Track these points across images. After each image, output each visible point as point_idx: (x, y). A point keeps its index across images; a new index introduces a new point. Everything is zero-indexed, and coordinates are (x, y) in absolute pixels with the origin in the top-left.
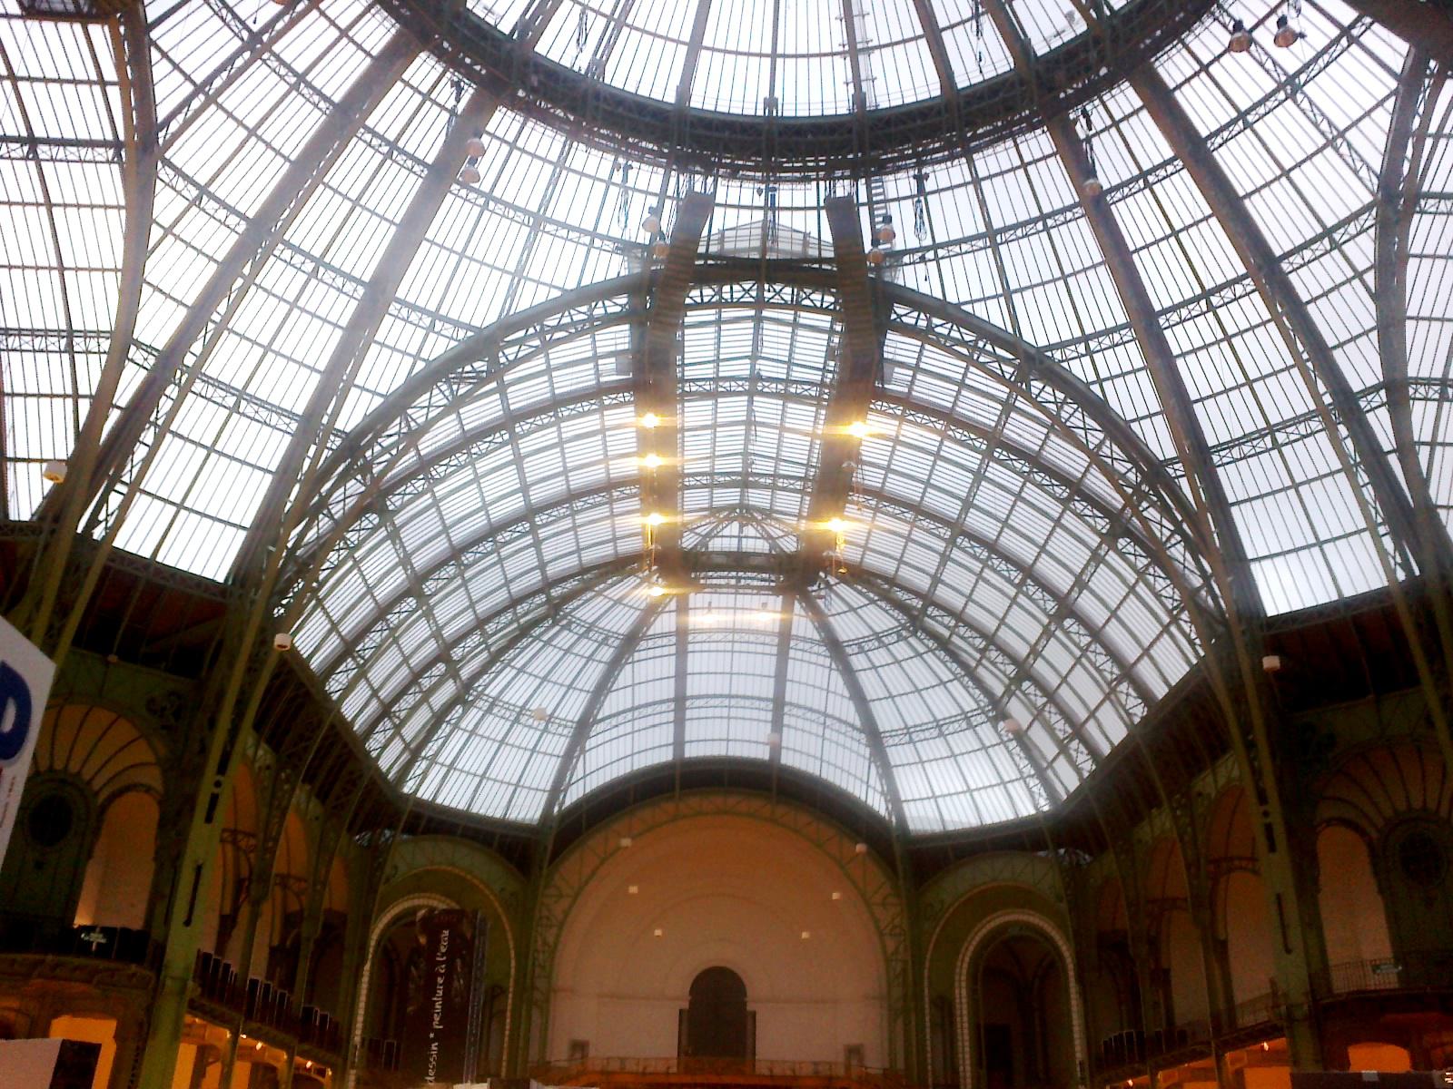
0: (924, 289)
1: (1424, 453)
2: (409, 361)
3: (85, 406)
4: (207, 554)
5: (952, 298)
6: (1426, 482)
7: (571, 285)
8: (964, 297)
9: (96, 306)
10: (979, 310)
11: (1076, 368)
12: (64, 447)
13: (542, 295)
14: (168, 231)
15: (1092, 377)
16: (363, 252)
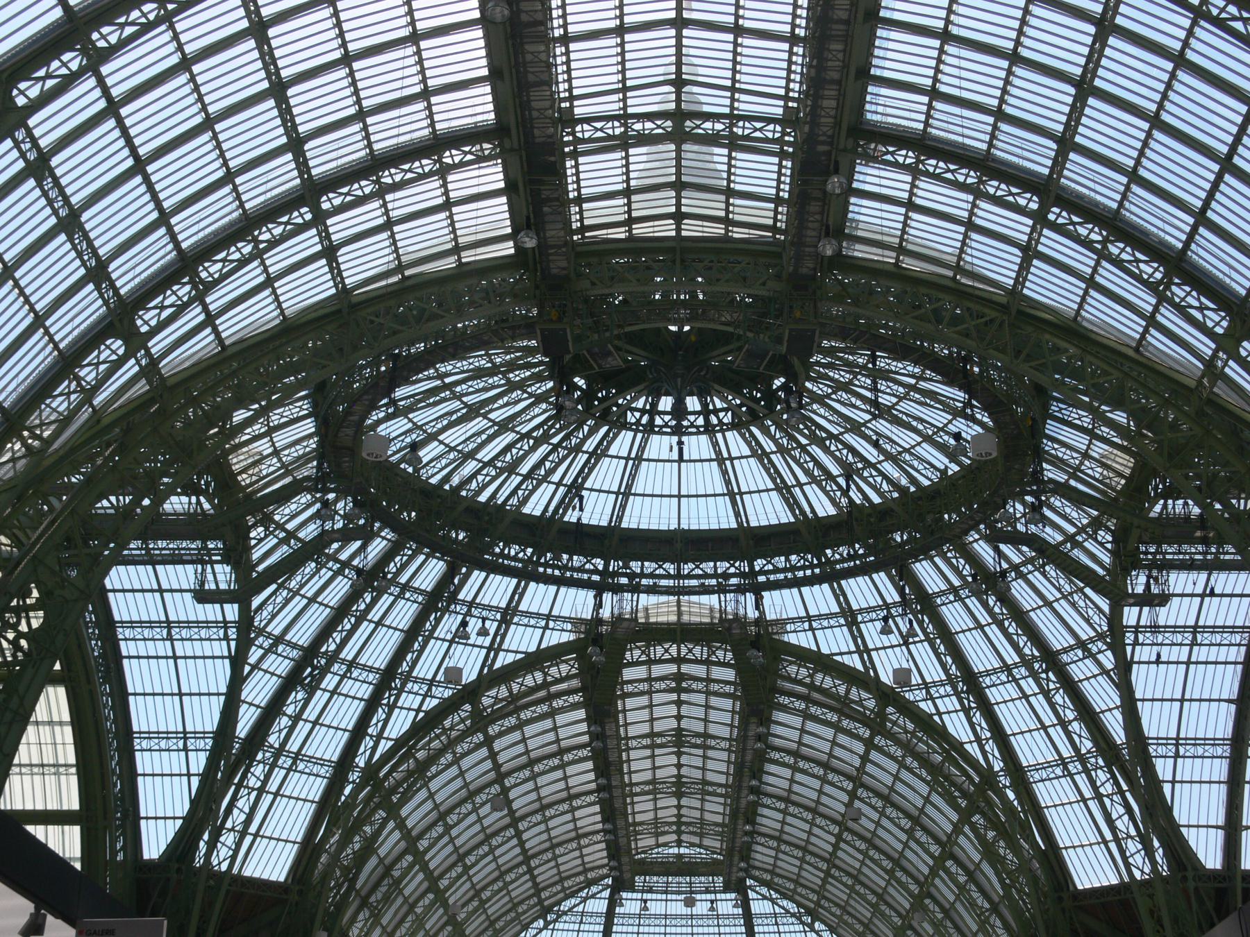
0: (804, 644)
1: (1167, 788)
2: (413, 713)
3: (195, 782)
4: (270, 863)
5: (825, 650)
6: (1171, 809)
7: (532, 648)
8: (835, 650)
9: (206, 716)
10: (846, 660)
11: (922, 705)
12: (183, 808)
13: (510, 658)
14: (255, 667)
15: (934, 711)
16: (380, 652)
